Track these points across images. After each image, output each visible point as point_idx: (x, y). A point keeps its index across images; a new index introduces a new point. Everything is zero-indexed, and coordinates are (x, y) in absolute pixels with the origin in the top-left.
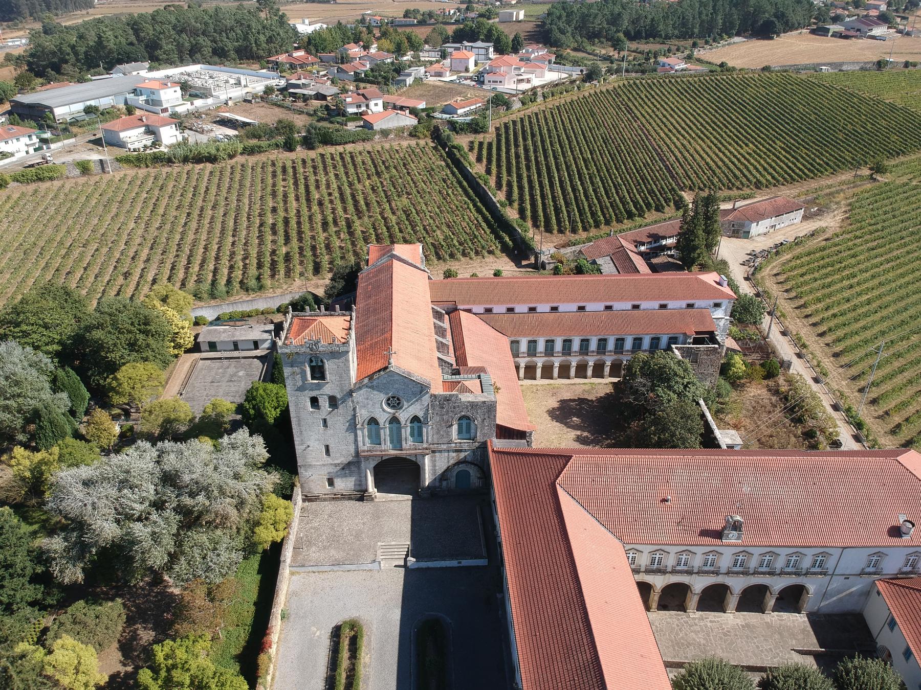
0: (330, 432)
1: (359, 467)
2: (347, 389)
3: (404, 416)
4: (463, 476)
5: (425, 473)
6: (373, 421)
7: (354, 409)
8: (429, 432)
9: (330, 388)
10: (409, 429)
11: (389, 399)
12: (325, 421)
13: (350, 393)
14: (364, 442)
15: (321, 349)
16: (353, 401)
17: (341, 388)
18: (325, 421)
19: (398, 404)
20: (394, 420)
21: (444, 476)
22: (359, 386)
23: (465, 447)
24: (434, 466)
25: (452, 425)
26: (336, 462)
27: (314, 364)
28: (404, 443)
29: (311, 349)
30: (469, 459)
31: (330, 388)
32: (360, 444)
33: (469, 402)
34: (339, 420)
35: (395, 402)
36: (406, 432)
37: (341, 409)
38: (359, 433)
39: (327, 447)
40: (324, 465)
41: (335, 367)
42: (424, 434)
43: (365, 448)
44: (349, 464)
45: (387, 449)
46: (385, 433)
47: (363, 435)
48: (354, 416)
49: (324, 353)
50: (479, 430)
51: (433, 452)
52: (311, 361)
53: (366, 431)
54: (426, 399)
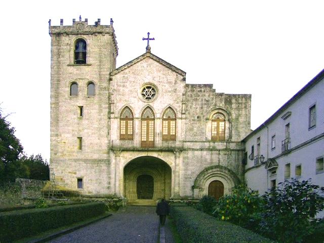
3: (159, 105)
4: (216, 187)
12: (81, 108)
18: (81, 108)
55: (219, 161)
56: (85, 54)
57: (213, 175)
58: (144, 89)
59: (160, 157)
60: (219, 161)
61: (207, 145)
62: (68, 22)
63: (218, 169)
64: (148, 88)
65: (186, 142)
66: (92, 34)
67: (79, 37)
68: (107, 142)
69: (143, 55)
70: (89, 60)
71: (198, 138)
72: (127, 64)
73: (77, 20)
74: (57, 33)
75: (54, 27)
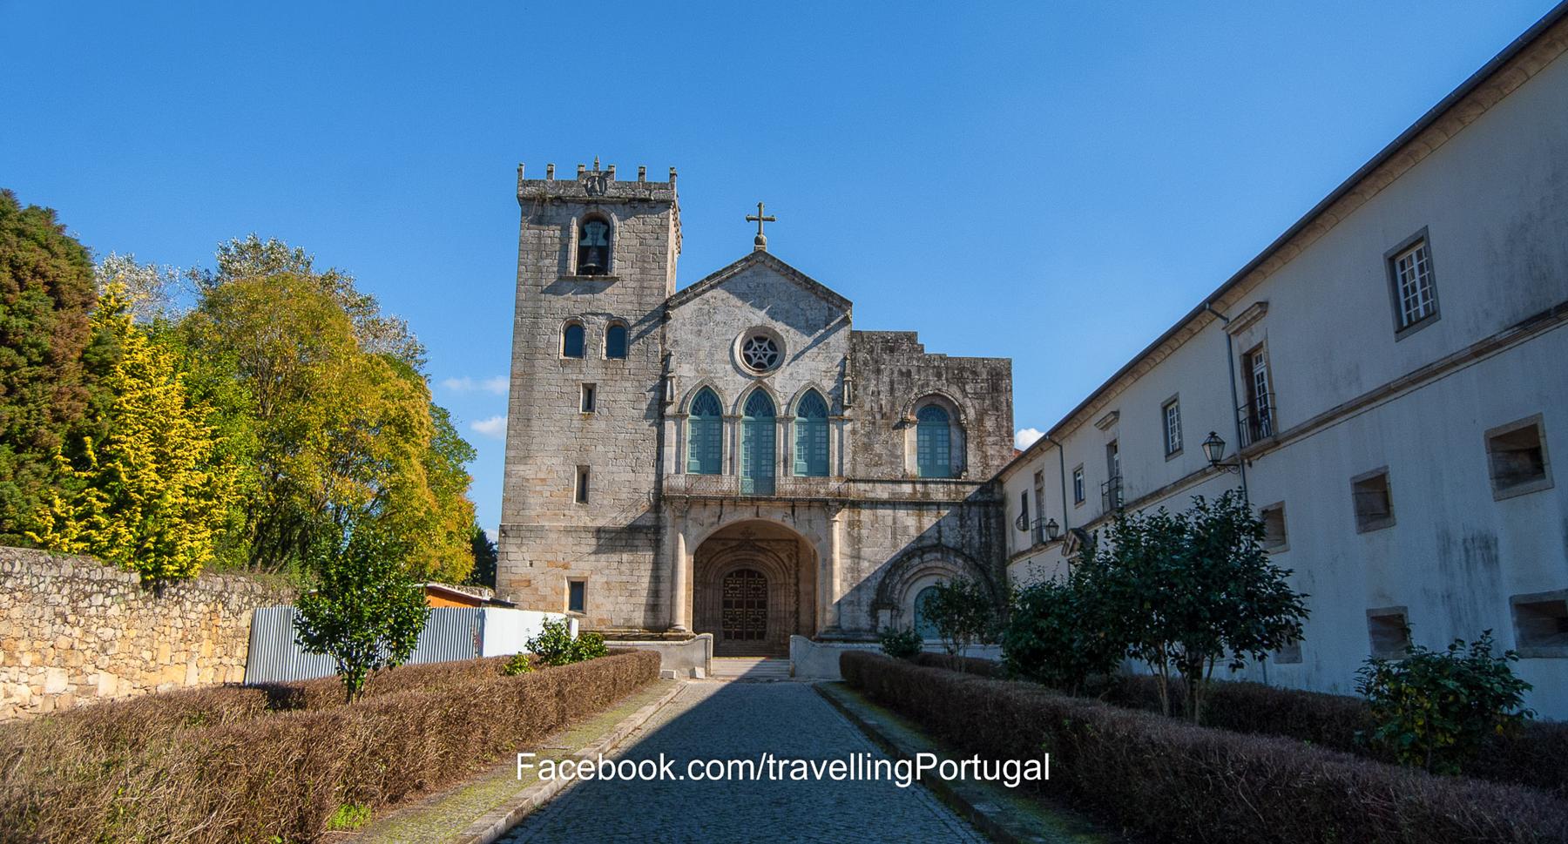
0: (598, 425)
1: (657, 546)
2: (654, 302)
3: (785, 384)
5: (830, 575)
6: (707, 402)
7: (666, 358)
8: (842, 439)
9: (615, 300)
10: (795, 433)
11: (747, 345)
12: (590, 391)
13: (662, 316)
14: (678, 463)
15: (611, 192)
16: (663, 337)
17: (641, 290)
18: (590, 391)
19: (772, 359)
20: (760, 403)
21: (881, 592)
22: (684, 296)
23: (939, 493)
24: (856, 557)
25: (903, 424)
26: (600, 523)
27: (588, 242)
28: (780, 470)
29: (590, 191)
30: (950, 538)
31: (615, 300)
32: (670, 466)
33: (942, 358)
34: (623, 396)
35: (763, 351)
36: (789, 438)
37: (631, 363)
38: (670, 427)
39: (584, 476)
40: (568, 531)
41: (636, 242)
42: (834, 447)
43: (680, 482)
44: (633, 530)
45: (735, 479)
46: (736, 438)
47: (679, 436)
48: (664, 379)
49: (615, 202)
50: (971, 446)
51: (855, 505)
52: (583, 235)
53: (688, 428)
54: (839, 340)
55: (939, 532)
56: (604, 255)
57: (924, 572)
58: (750, 342)
59: (789, 523)
60: (939, 532)
61: (907, 489)
62: (565, 172)
63: (939, 555)
64: (760, 339)
65: (854, 481)
66: (624, 204)
67: (593, 209)
68: (653, 478)
69: (746, 259)
70: (617, 266)
71: (885, 471)
72: (708, 279)
73: (588, 167)
74: (539, 206)
75: (530, 183)
